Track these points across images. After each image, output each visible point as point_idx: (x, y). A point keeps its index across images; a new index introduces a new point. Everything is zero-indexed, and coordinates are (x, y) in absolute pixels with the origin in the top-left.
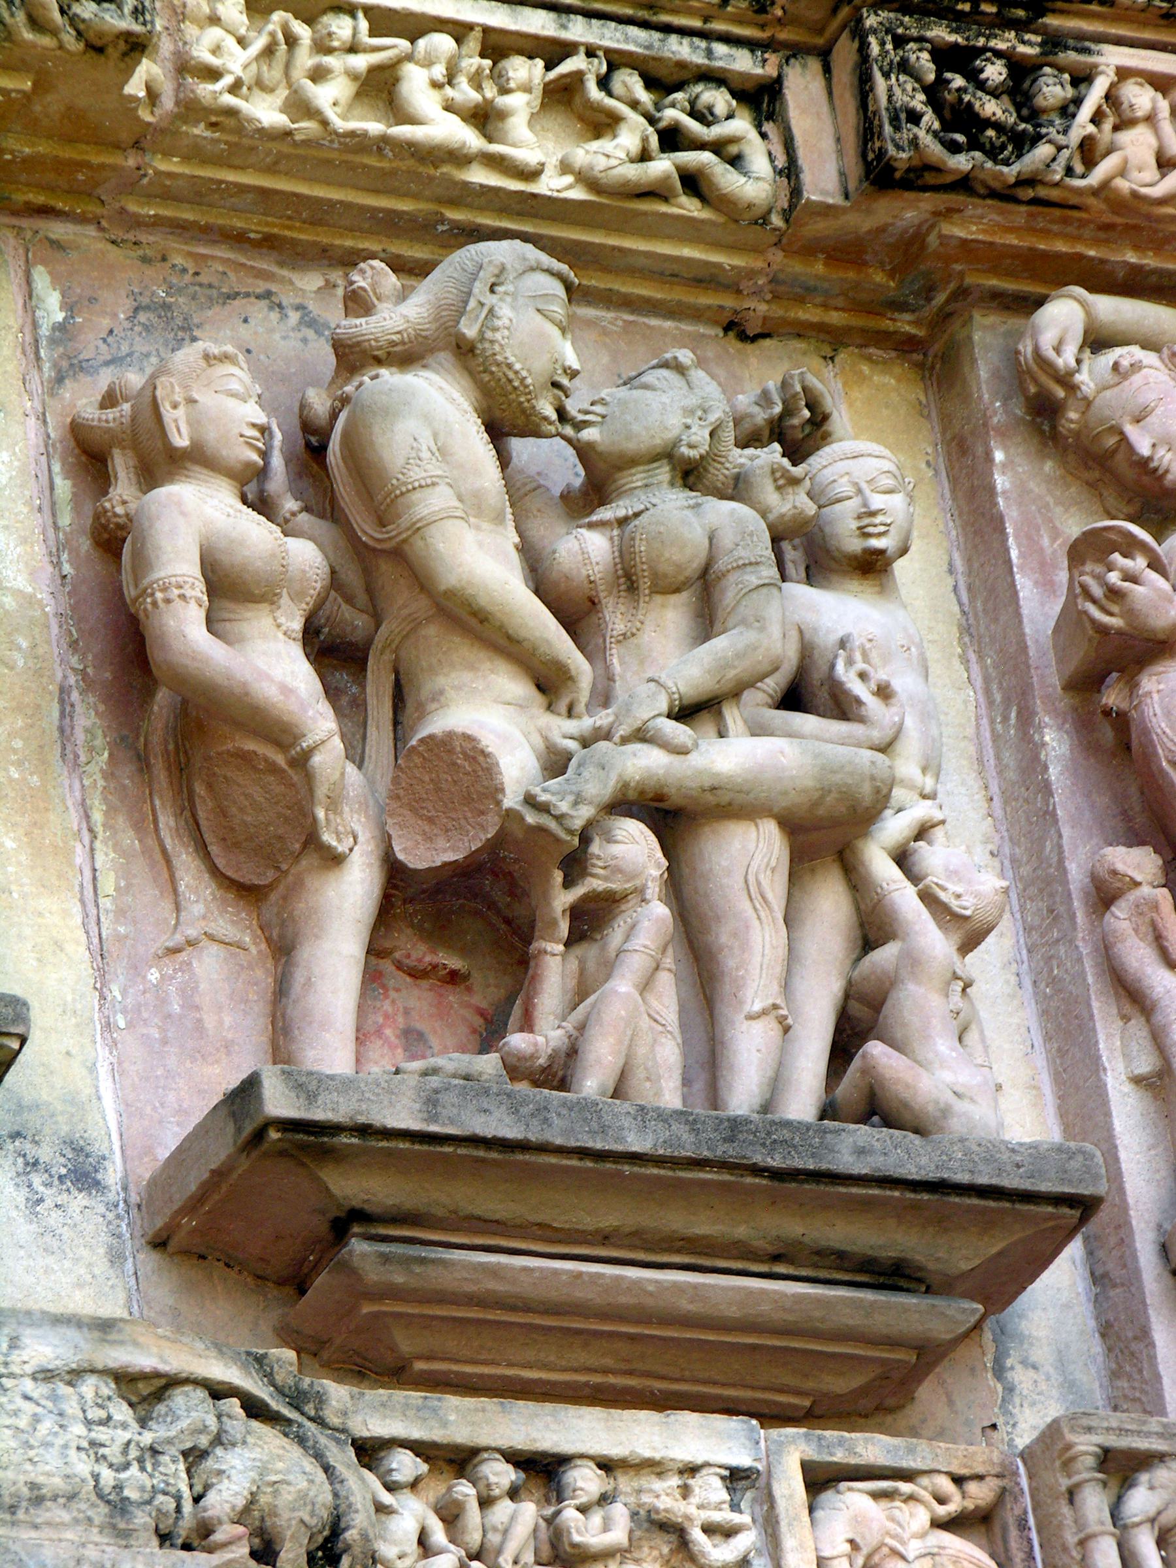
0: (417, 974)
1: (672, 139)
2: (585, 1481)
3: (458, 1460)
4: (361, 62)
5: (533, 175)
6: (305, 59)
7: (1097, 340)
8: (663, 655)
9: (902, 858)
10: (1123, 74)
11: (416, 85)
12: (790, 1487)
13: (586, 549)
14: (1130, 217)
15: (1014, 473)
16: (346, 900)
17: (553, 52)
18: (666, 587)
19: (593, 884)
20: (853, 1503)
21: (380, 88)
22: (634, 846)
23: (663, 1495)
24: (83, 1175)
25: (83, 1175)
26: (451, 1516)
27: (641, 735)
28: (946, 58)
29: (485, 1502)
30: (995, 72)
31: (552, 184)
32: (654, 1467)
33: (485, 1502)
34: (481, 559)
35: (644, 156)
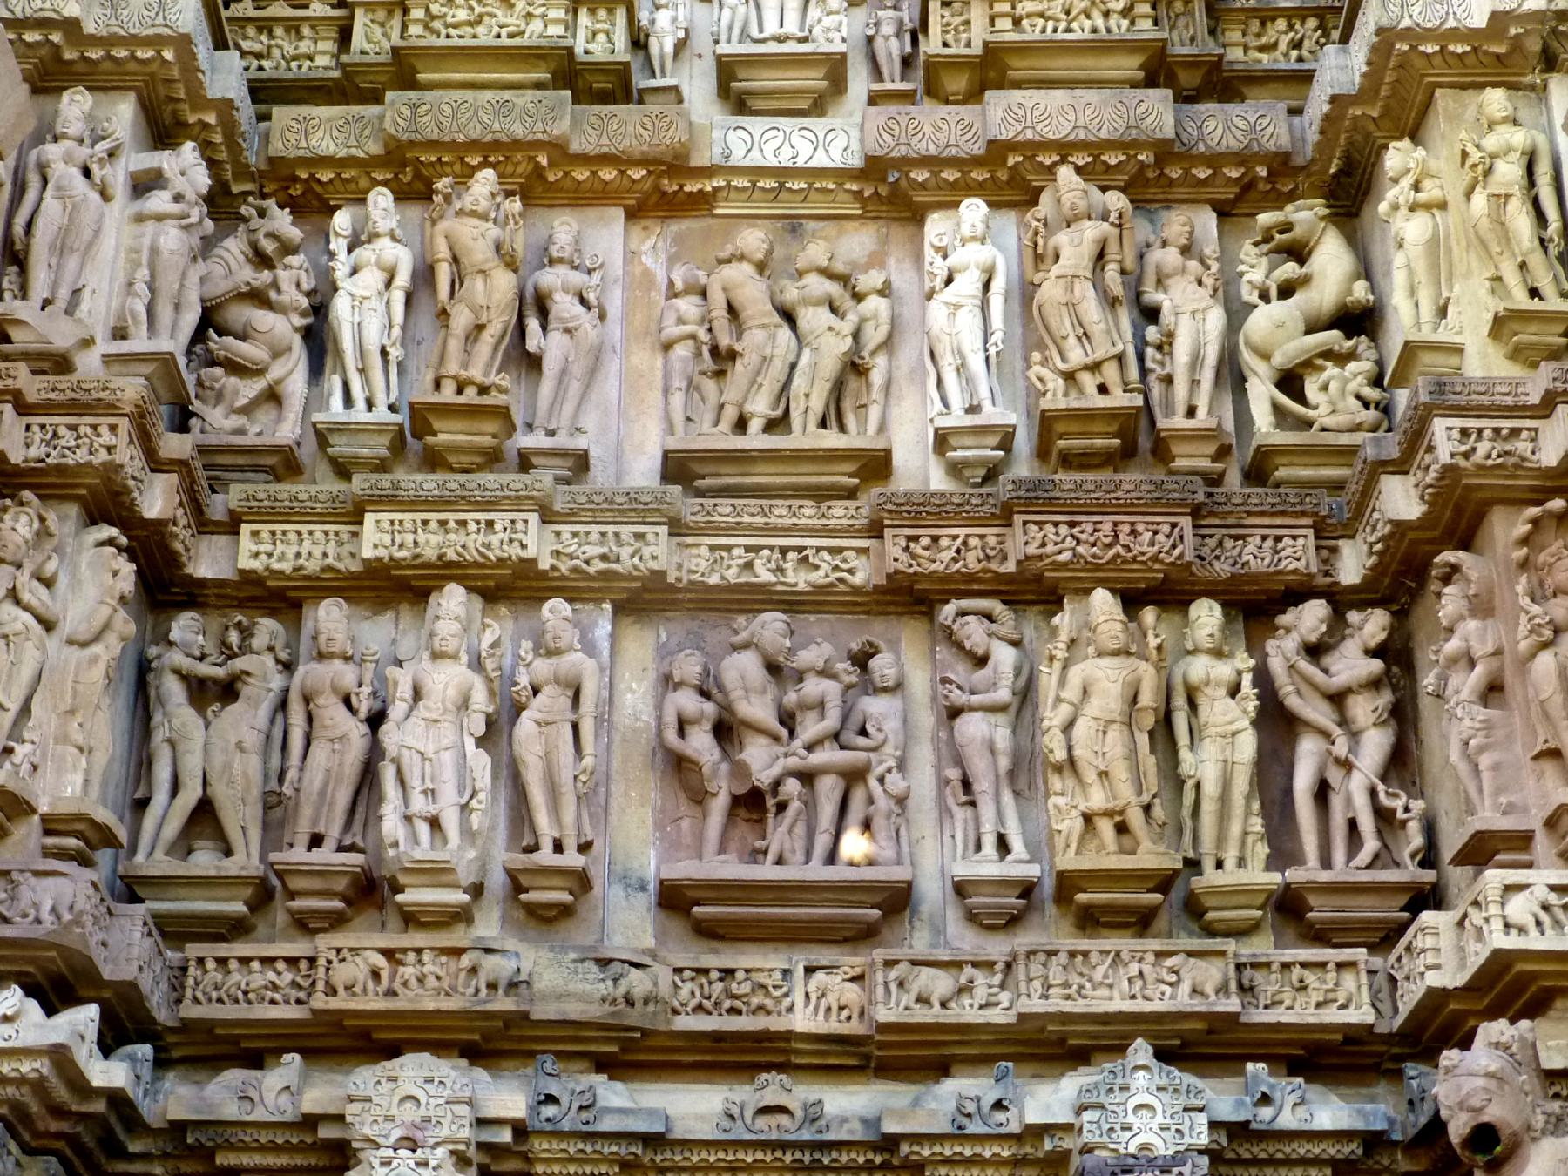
0: (747, 821)
1: (836, 568)
2: (740, 975)
3: (706, 971)
4: (741, 561)
5: (796, 585)
6: (726, 562)
7: (963, 613)
8: (810, 728)
9: (881, 780)
10: (967, 536)
11: (758, 563)
12: (800, 971)
13: (791, 698)
14: (971, 578)
15: (943, 652)
16: (719, 806)
17: (800, 549)
18: (810, 708)
19: (780, 798)
20: (820, 976)
21: (749, 566)
22: (792, 786)
23: (761, 978)
24: (643, 888)
25: (643, 888)
26: (702, 986)
27: (794, 754)
28: (910, 538)
29: (710, 983)
30: (925, 541)
31: (802, 586)
32: (760, 970)
33: (710, 983)
34: (757, 708)
35: (827, 576)
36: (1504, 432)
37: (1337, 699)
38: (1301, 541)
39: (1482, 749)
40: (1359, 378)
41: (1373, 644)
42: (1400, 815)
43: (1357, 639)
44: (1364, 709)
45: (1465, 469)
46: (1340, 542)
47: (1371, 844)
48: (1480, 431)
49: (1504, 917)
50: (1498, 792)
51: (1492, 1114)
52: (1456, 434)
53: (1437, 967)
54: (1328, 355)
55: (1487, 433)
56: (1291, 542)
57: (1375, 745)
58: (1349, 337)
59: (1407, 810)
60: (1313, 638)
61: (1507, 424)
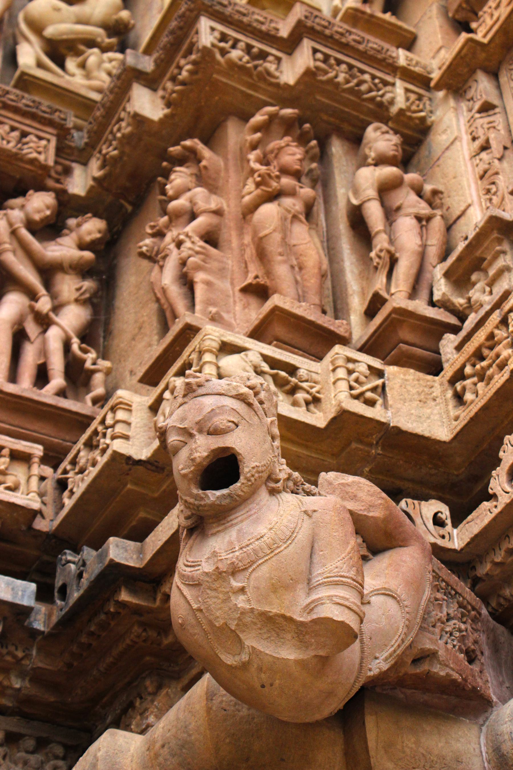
36: (255, 50)
37: (48, 272)
38: (44, 143)
39: (198, 268)
40: (114, 63)
41: (88, 239)
42: (88, 365)
43: (74, 235)
44: (68, 286)
45: (219, 63)
46: (74, 165)
47: (57, 381)
48: (236, 41)
49: (218, 368)
50: (209, 302)
51: (236, 441)
52: (217, 34)
53: (127, 438)
54: (91, 43)
55: (241, 45)
56: (35, 139)
57: (73, 318)
58: (109, 36)
59: (94, 364)
60: (37, 217)
61: (258, 46)
